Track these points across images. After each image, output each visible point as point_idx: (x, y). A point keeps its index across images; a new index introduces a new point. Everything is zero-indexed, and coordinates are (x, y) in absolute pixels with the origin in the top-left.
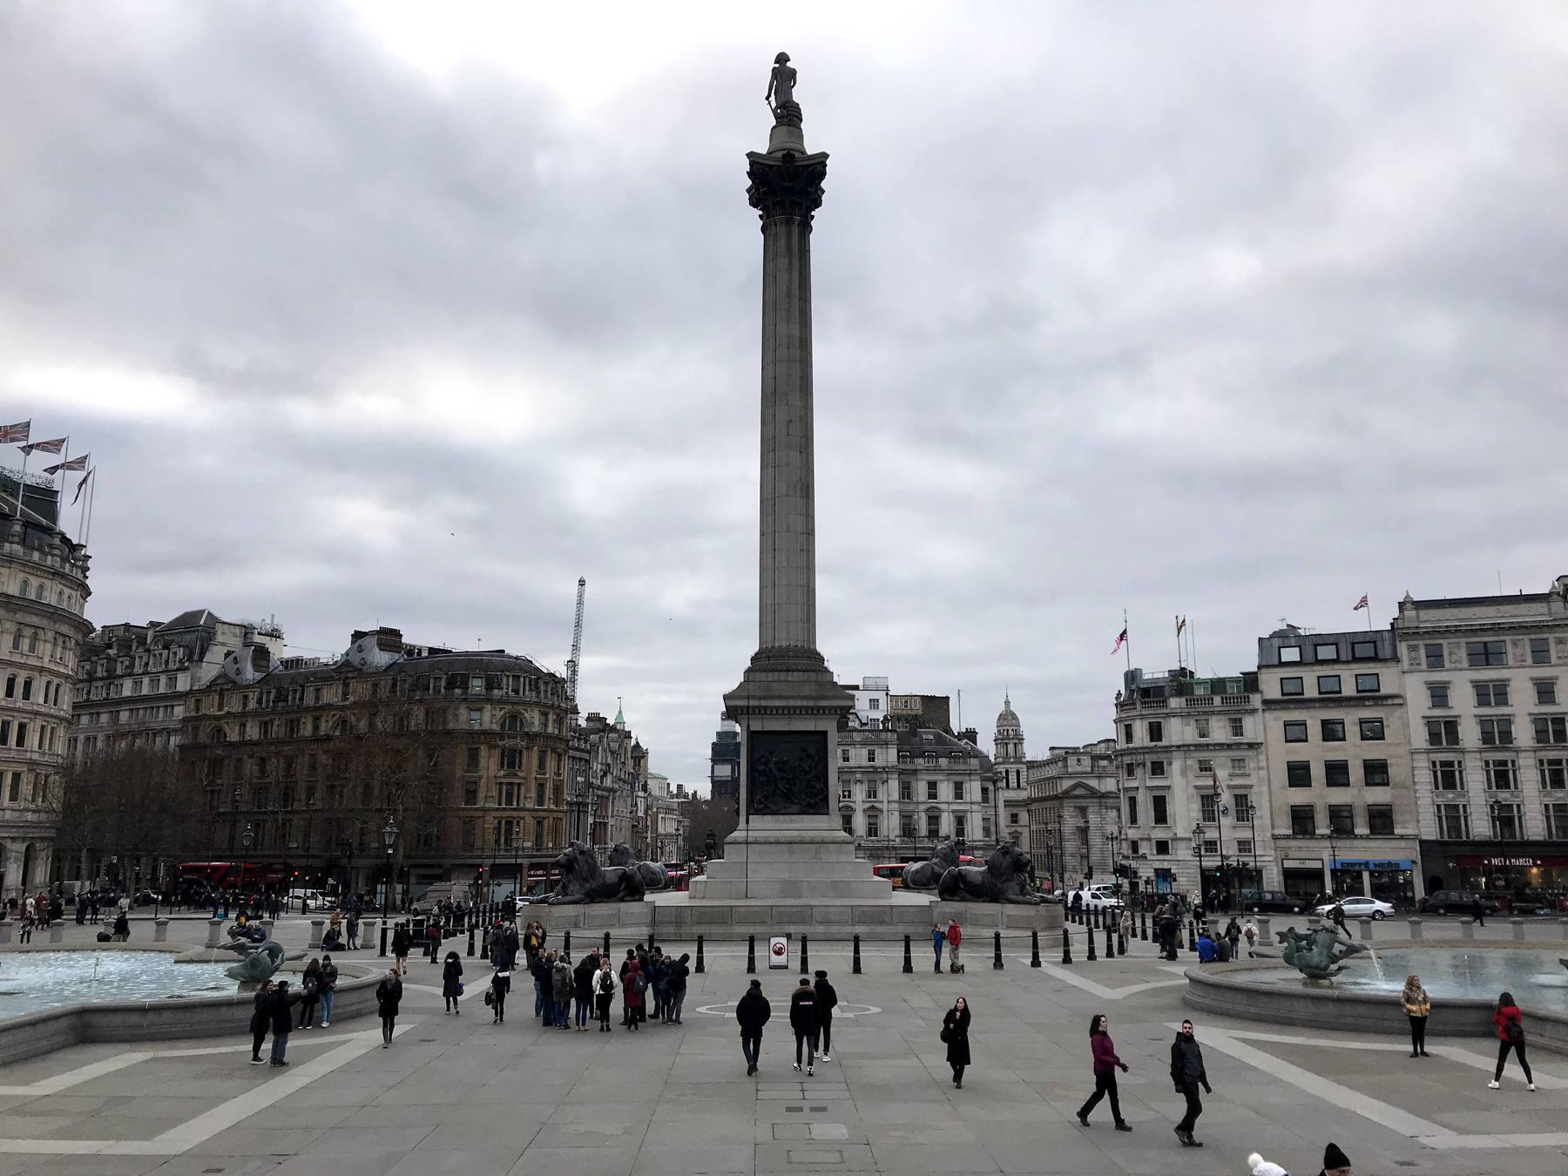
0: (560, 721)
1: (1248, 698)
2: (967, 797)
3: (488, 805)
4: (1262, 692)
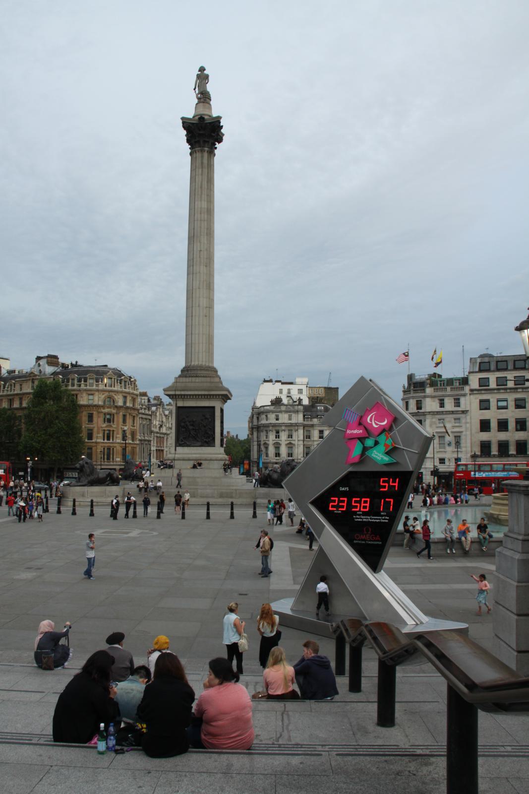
0: (134, 400)
1: (463, 388)
3: (99, 440)
4: (469, 385)
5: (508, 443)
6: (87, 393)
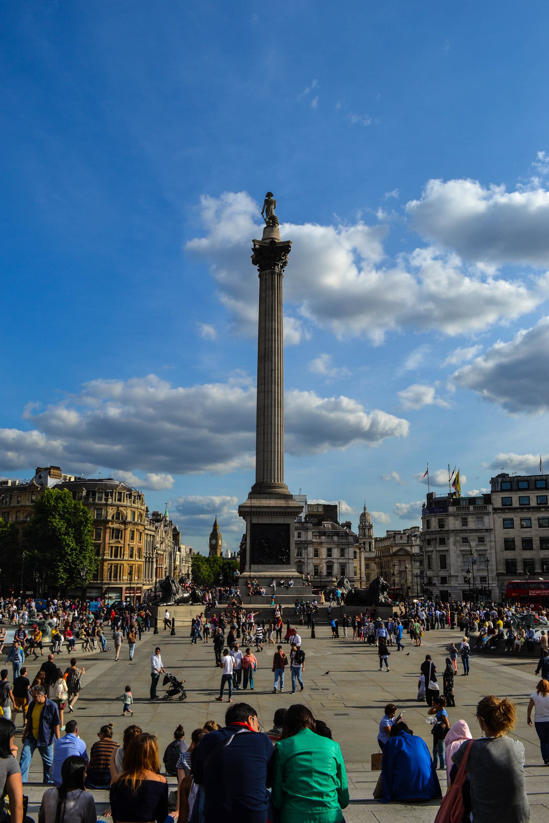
2: (346, 556)
3: (105, 557)
4: (493, 504)
5: (516, 562)
6: (95, 508)
